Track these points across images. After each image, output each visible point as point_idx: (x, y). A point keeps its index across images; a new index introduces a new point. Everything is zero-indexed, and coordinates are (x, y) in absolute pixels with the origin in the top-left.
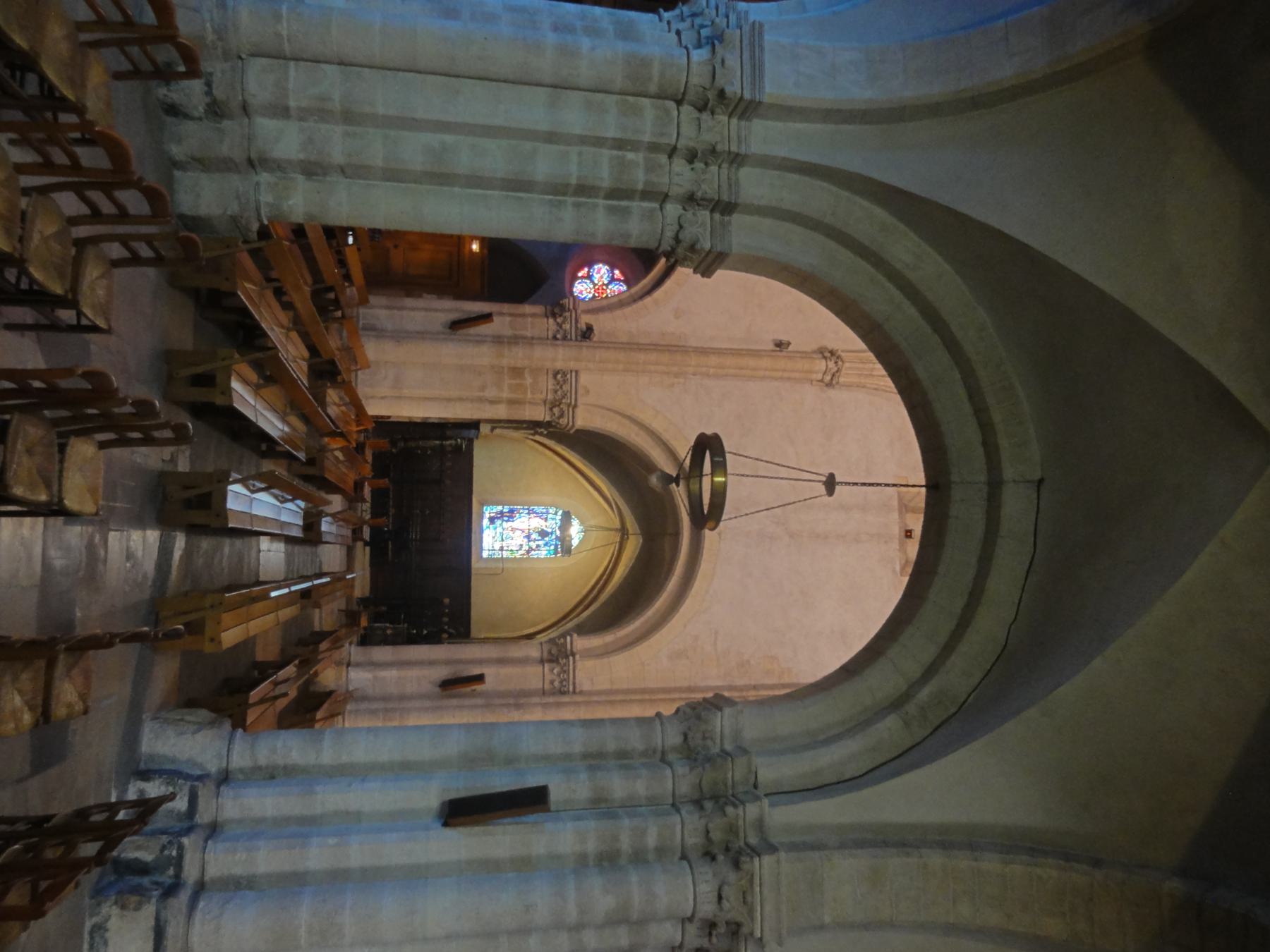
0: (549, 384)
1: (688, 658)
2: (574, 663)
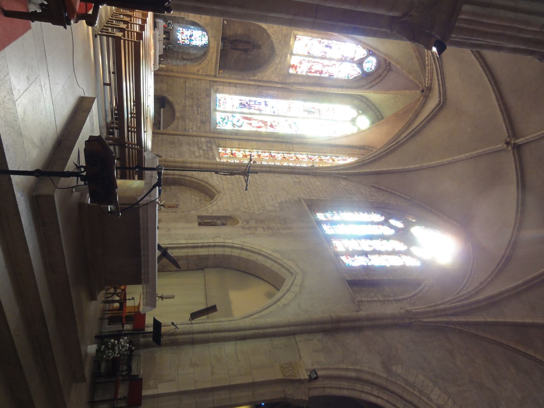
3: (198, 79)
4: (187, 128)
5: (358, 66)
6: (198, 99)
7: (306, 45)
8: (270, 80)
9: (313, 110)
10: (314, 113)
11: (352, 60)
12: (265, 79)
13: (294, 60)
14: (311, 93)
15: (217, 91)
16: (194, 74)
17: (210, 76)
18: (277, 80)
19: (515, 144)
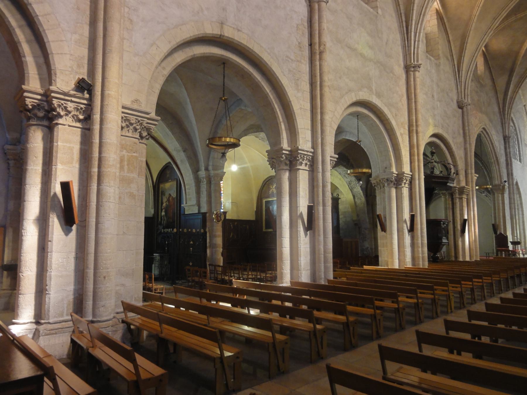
0: (127, 134)
1: (298, 80)
2: (303, 150)
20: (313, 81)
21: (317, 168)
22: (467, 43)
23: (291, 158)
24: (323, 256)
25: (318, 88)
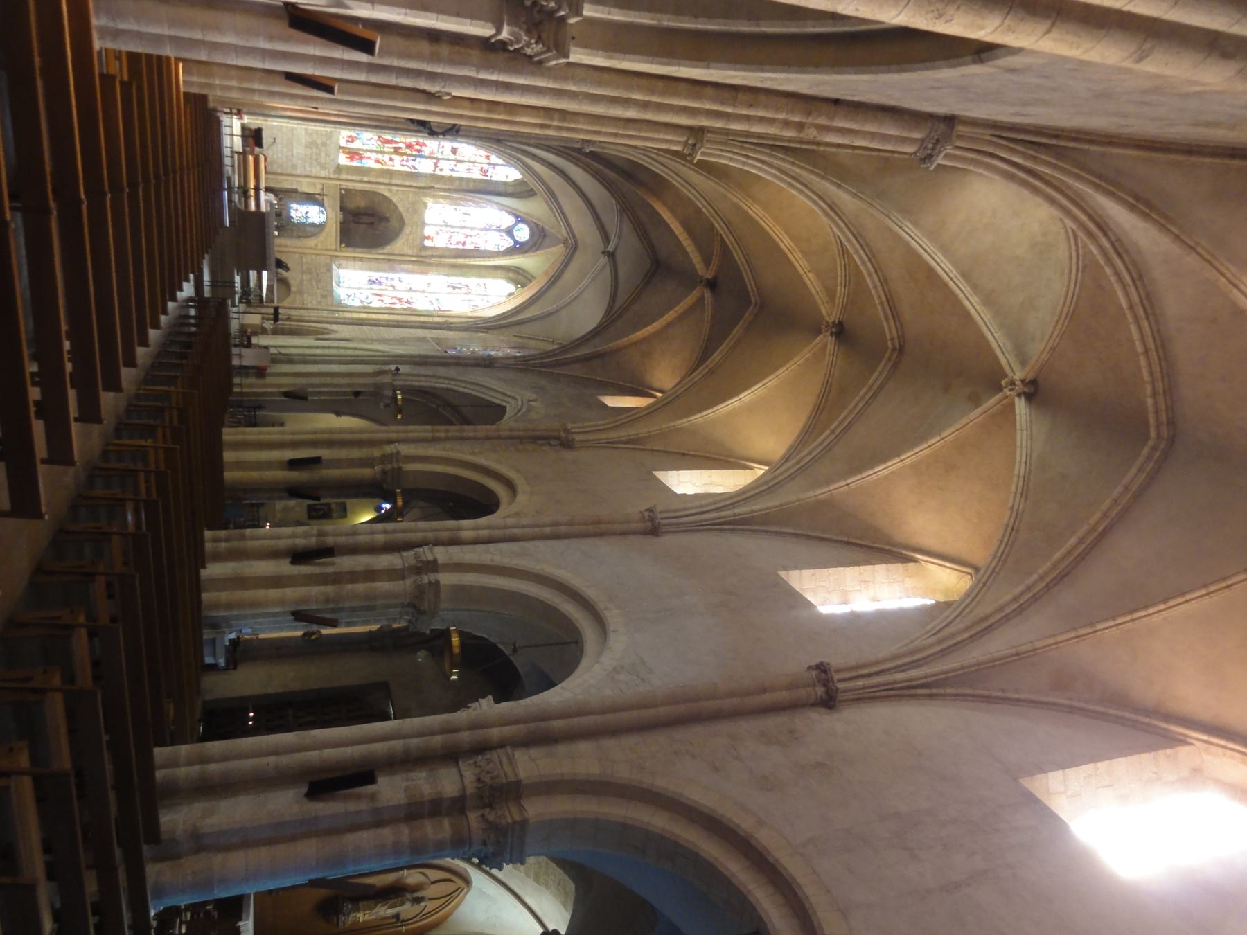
3: (317, 255)
4: (305, 302)
5: (507, 235)
6: (317, 274)
7: (440, 214)
8: (402, 253)
9: (460, 286)
10: (460, 288)
11: (499, 229)
12: (396, 252)
13: (428, 231)
14: (454, 266)
15: (339, 267)
16: (311, 248)
17: (330, 250)
18: (410, 252)
19: (608, 252)
20: (740, 96)
21: (490, 67)
22: (707, 178)
23: (540, 12)
24: (198, 35)
25: (715, 107)
